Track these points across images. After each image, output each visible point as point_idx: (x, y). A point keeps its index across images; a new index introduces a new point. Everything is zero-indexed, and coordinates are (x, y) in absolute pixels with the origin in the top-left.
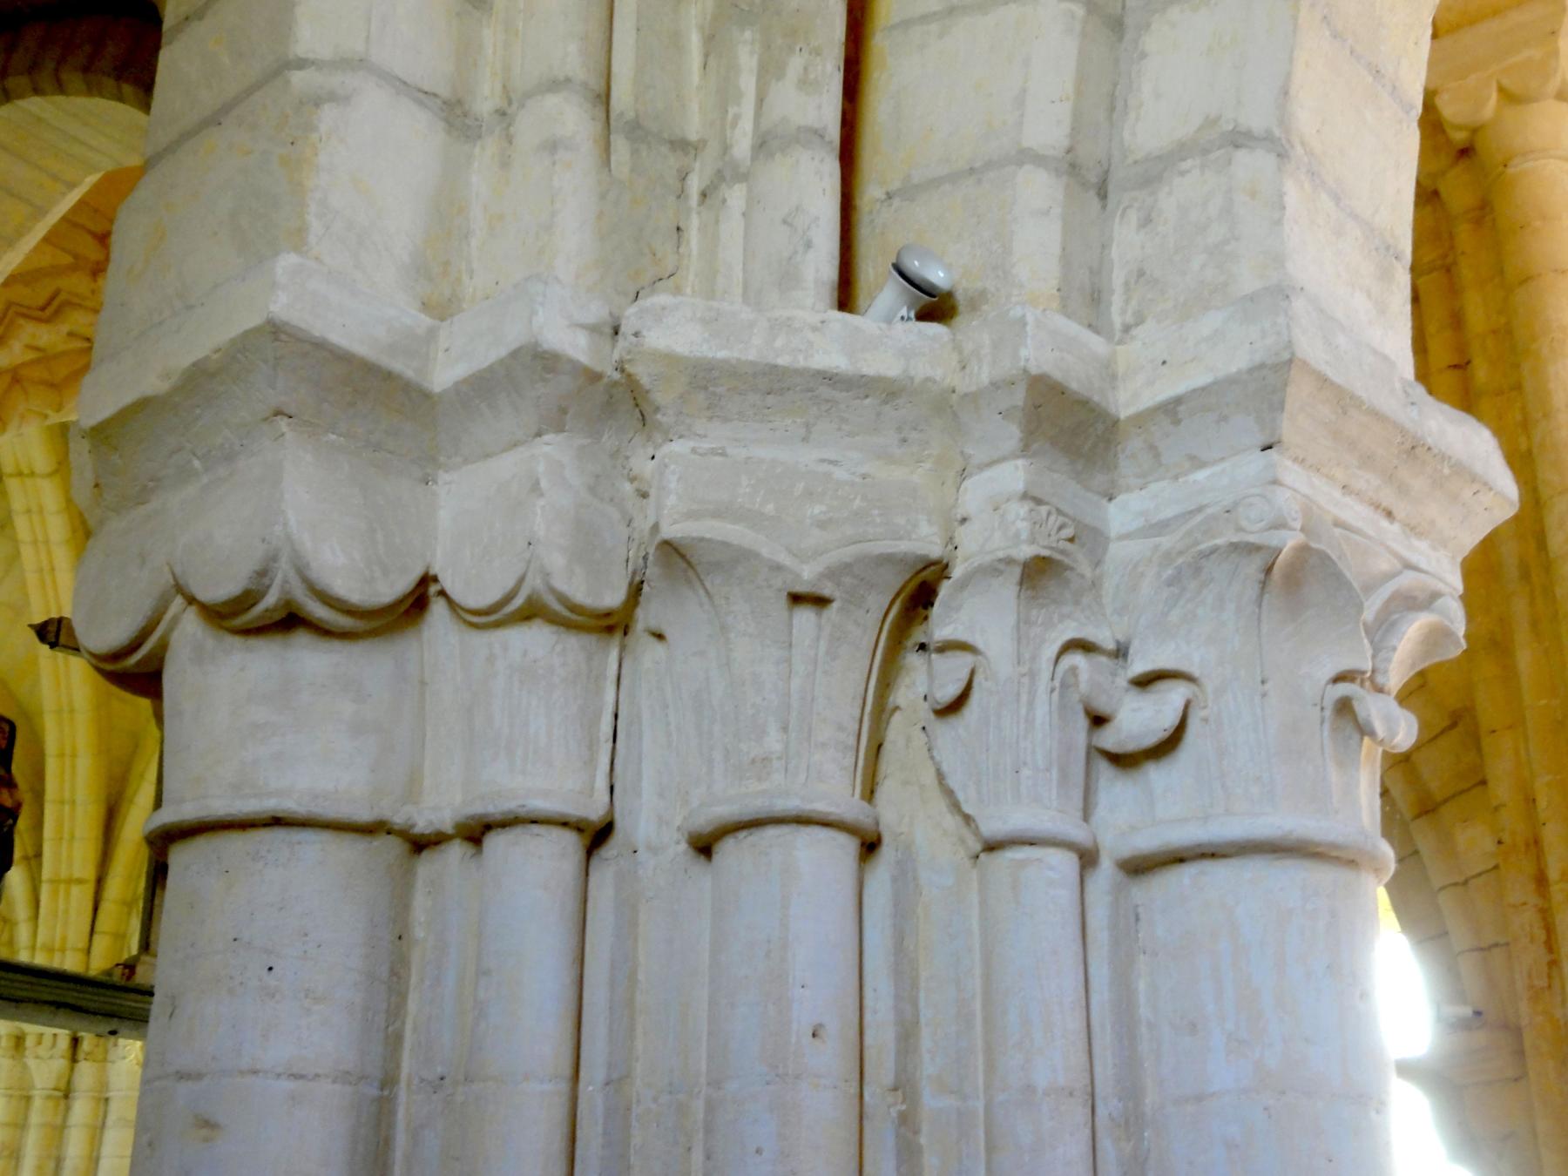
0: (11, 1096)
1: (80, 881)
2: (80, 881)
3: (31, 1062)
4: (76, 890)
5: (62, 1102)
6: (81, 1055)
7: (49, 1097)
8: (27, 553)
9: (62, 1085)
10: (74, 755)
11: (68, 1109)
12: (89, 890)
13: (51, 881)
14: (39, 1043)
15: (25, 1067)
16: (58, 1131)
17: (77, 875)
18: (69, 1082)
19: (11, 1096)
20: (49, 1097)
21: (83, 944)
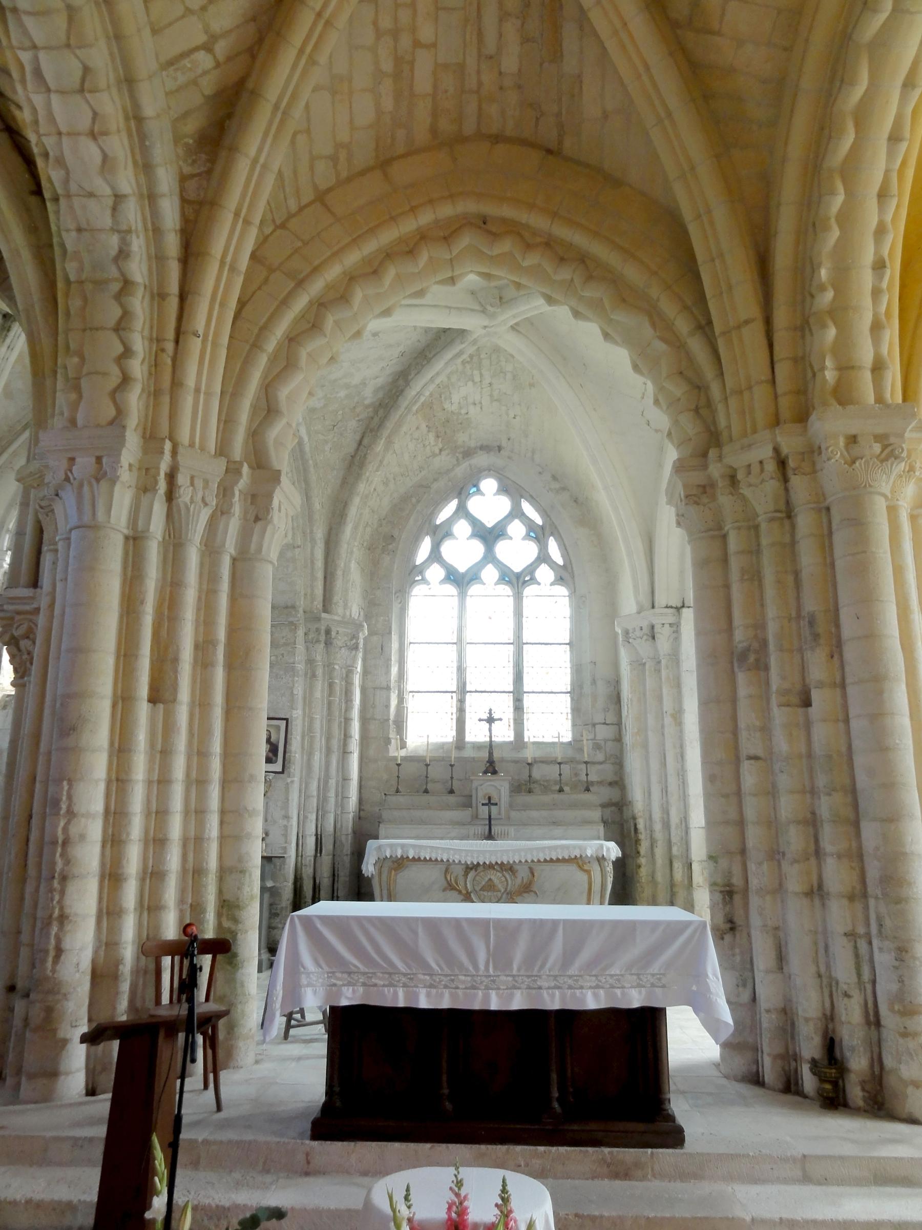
0: (739, 528)
1: (747, 322)
2: (747, 322)
3: (745, 491)
4: (746, 331)
5: (787, 522)
6: (790, 473)
7: (772, 520)
8: (596, 18)
9: (783, 507)
10: (709, 211)
11: (793, 527)
12: (758, 327)
13: (723, 333)
14: (749, 473)
15: (744, 498)
16: (790, 547)
17: (743, 316)
18: (788, 503)
19: (739, 528)
20: (772, 520)
21: (765, 374)
